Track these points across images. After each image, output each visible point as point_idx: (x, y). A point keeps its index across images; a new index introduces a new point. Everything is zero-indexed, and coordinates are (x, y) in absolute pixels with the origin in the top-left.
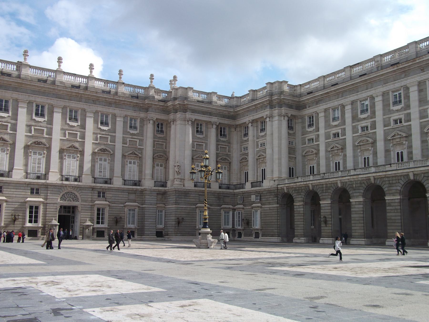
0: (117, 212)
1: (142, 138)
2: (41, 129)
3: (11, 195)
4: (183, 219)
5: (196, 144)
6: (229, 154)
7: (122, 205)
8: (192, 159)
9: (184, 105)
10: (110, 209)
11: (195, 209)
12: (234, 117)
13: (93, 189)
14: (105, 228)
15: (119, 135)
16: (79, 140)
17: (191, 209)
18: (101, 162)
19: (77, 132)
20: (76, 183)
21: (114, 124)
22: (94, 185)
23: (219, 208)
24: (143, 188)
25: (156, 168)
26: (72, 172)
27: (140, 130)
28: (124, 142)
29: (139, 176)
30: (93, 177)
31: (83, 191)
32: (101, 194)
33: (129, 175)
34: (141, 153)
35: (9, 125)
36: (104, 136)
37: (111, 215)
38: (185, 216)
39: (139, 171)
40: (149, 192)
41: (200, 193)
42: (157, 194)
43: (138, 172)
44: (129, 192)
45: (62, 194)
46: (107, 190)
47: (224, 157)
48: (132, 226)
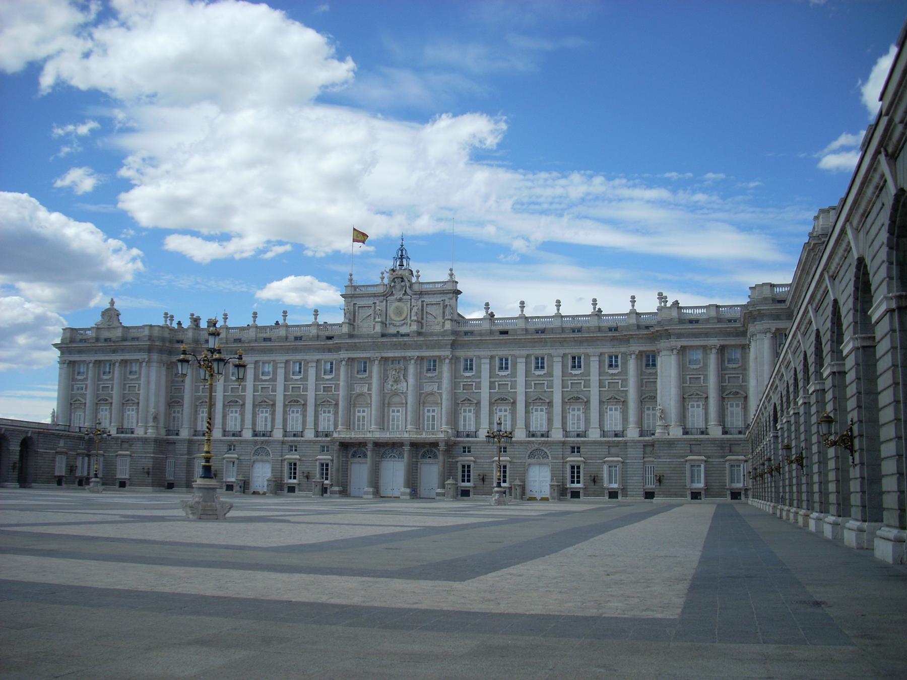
0: (594, 470)
1: (625, 377)
2: (506, 384)
3: (478, 456)
4: (663, 476)
5: (690, 378)
6: (745, 385)
7: (601, 461)
8: (683, 398)
9: (666, 330)
10: (586, 467)
11: (684, 463)
12: (744, 334)
13: (564, 443)
14: (580, 488)
15: (594, 378)
16: (547, 390)
17: (677, 463)
18: (574, 412)
19: (544, 382)
20: (543, 439)
22: (563, 439)
23: (722, 460)
24: (624, 439)
25: (647, 412)
26: (540, 426)
27: (622, 368)
28: (601, 385)
29: (623, 425)
30: (565, 430)
31: (553, 447)
32: (575, 449)
33: (610, 424)
34: (626, 395)
35: (474, 384)
36: (576, 381)
37: (585, 472)
38: (669, 472)
39: (623, 419)
40: (633, 444)
41: (691, 443)
42: (644, 445)
43: (621, 420)
44: (609, 445)
45: (529, 452)
46: (581, 444)
47: (734, 390)
48: (615, 486)
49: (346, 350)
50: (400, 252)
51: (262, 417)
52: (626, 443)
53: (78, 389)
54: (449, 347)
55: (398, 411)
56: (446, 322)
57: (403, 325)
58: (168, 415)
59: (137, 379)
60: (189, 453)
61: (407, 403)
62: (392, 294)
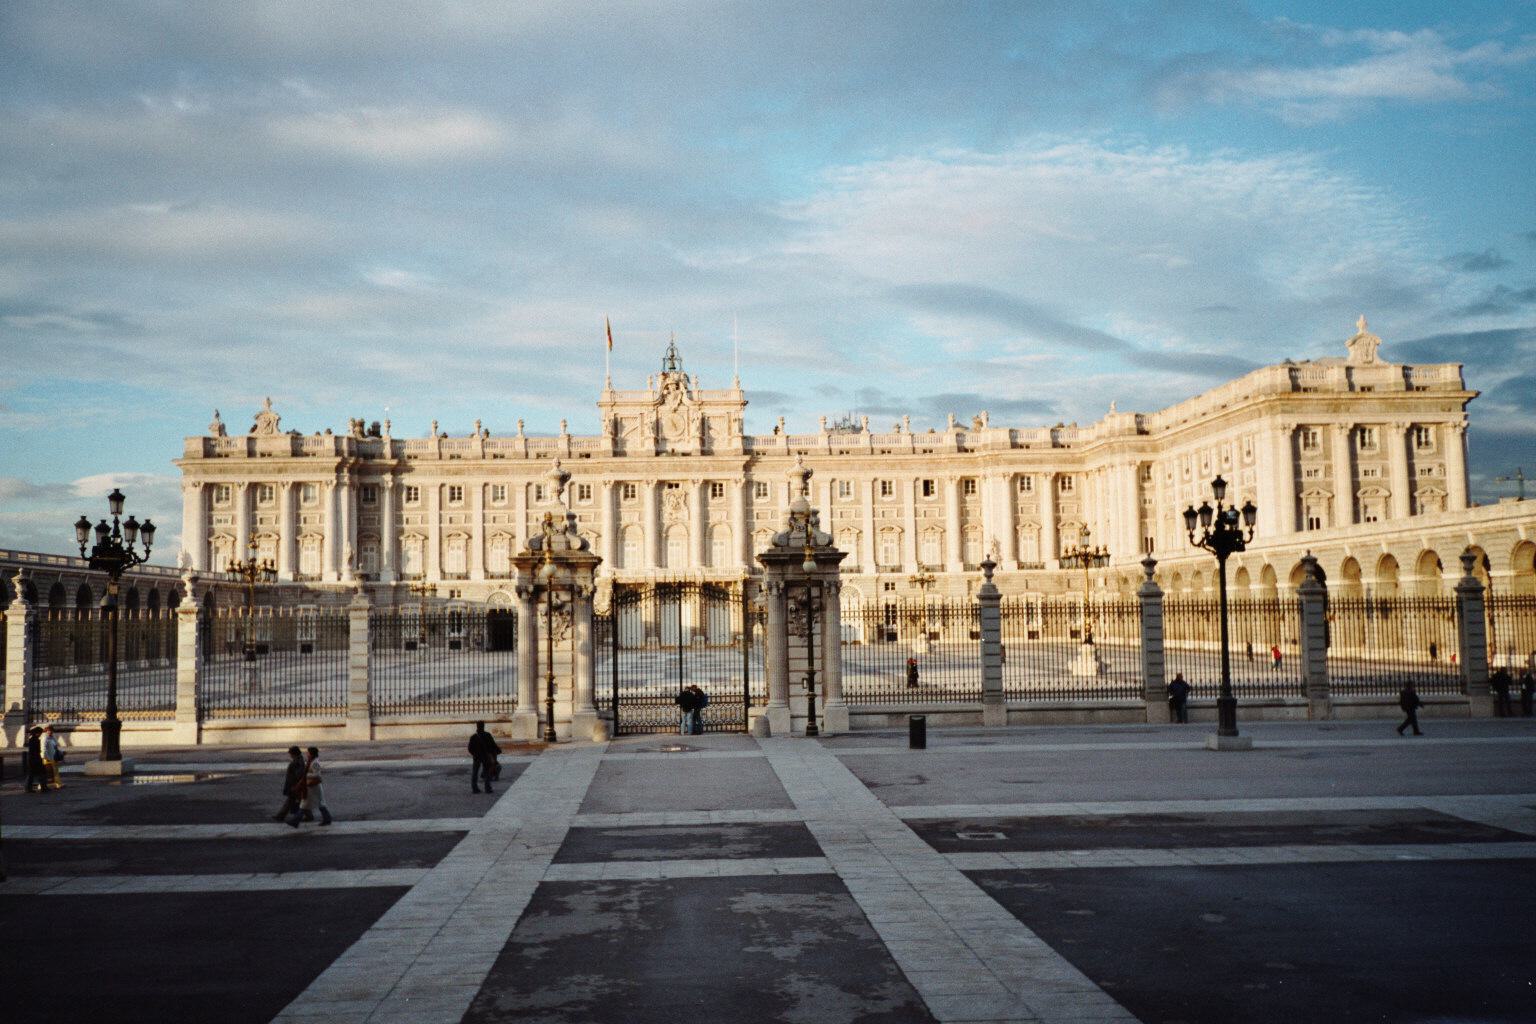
18: (886, 545)
21: (900, 491)
22: (877, 575)
49: (611, 471)
50: (670, 353)
51: (497, 554)
52: (946, 580)
53: (220, 521)
54: (741, 469)
55: (678, 544)
56: (733, 440)
57: (679, 441)
58: (359, 552)
59: (316, 508)
60: (396, 603)
61: (689, 535)
62: (662, 402)
